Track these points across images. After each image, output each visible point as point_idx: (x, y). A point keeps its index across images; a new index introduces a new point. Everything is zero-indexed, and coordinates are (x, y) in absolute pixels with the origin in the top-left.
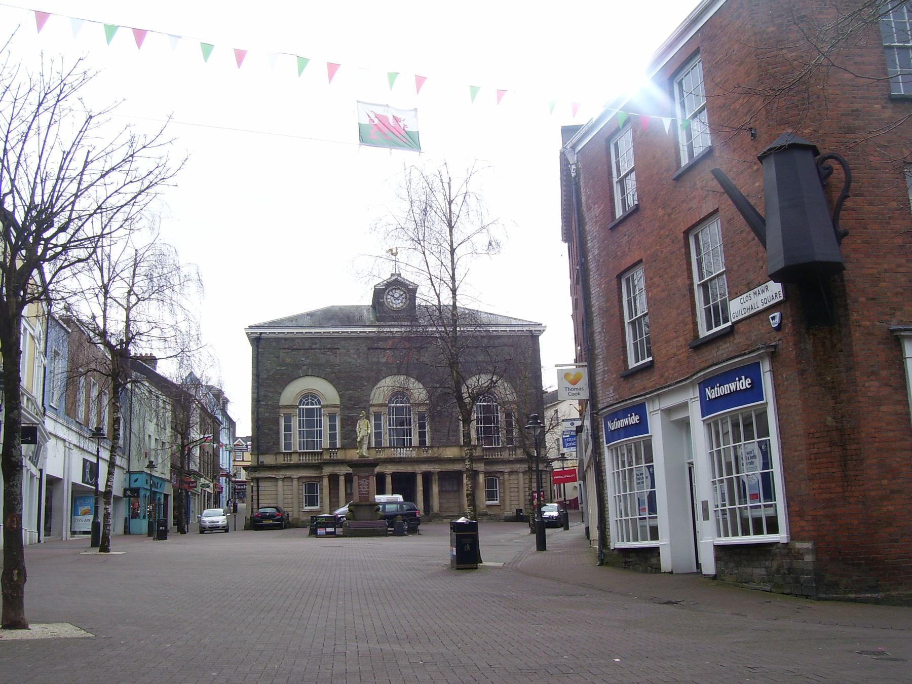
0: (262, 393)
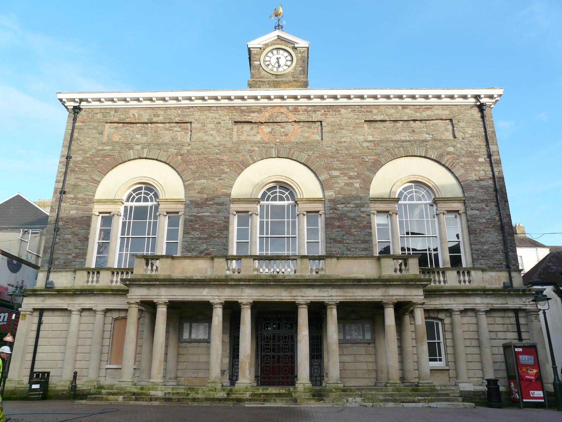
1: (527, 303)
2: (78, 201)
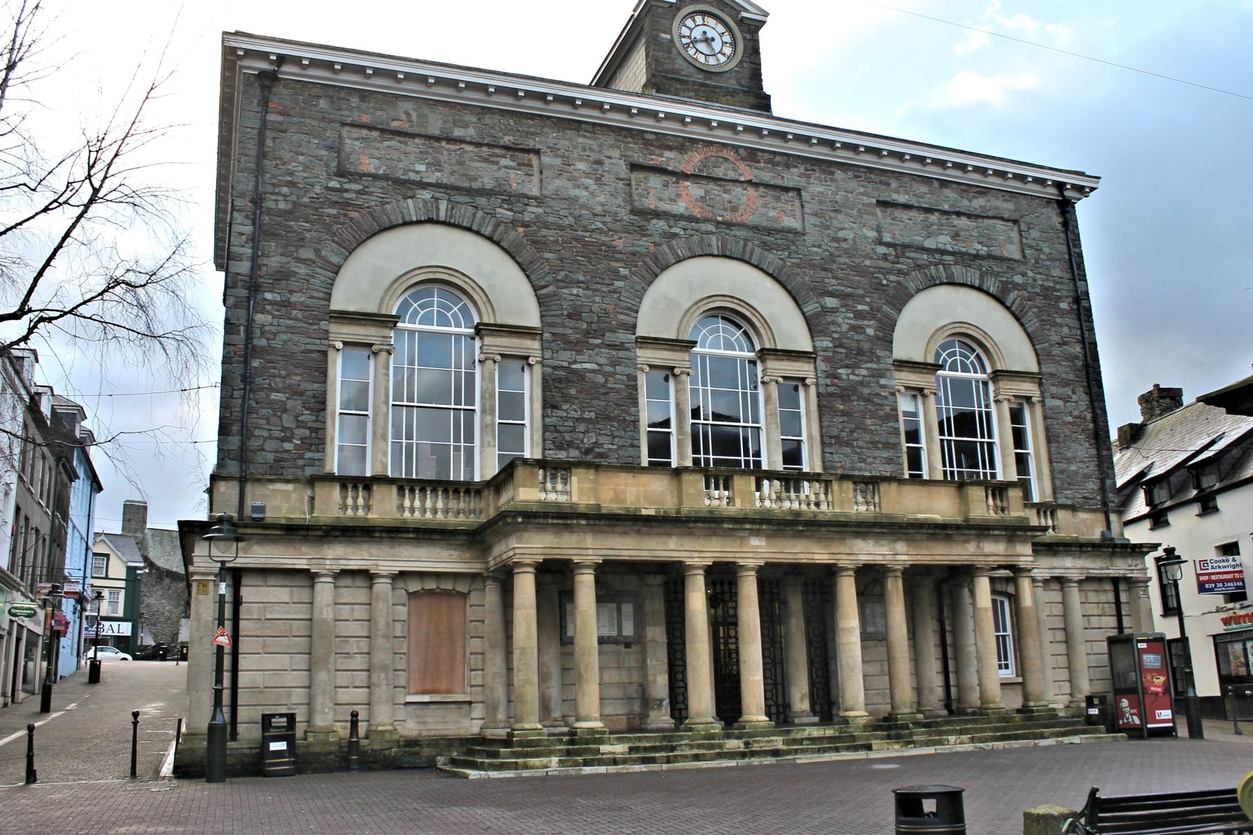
0: (274, 261)
1: (1133, 568)
2: (294, 312)
